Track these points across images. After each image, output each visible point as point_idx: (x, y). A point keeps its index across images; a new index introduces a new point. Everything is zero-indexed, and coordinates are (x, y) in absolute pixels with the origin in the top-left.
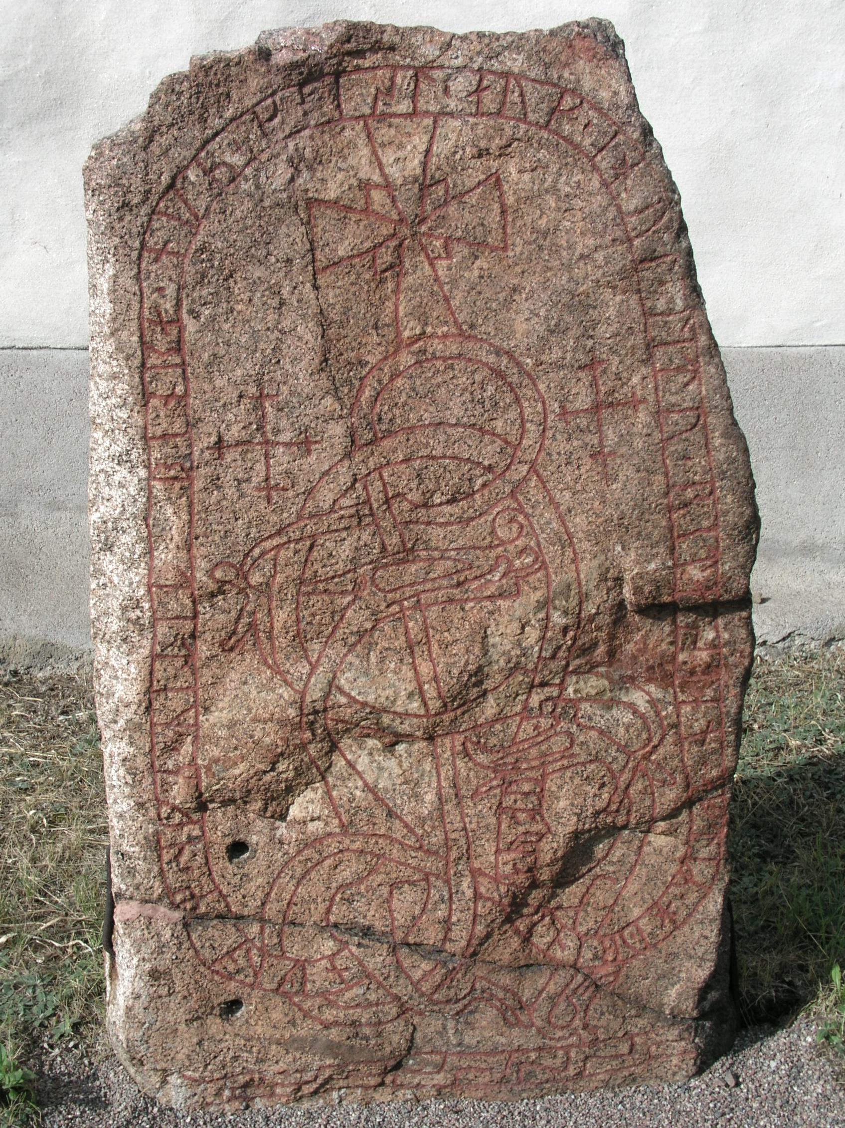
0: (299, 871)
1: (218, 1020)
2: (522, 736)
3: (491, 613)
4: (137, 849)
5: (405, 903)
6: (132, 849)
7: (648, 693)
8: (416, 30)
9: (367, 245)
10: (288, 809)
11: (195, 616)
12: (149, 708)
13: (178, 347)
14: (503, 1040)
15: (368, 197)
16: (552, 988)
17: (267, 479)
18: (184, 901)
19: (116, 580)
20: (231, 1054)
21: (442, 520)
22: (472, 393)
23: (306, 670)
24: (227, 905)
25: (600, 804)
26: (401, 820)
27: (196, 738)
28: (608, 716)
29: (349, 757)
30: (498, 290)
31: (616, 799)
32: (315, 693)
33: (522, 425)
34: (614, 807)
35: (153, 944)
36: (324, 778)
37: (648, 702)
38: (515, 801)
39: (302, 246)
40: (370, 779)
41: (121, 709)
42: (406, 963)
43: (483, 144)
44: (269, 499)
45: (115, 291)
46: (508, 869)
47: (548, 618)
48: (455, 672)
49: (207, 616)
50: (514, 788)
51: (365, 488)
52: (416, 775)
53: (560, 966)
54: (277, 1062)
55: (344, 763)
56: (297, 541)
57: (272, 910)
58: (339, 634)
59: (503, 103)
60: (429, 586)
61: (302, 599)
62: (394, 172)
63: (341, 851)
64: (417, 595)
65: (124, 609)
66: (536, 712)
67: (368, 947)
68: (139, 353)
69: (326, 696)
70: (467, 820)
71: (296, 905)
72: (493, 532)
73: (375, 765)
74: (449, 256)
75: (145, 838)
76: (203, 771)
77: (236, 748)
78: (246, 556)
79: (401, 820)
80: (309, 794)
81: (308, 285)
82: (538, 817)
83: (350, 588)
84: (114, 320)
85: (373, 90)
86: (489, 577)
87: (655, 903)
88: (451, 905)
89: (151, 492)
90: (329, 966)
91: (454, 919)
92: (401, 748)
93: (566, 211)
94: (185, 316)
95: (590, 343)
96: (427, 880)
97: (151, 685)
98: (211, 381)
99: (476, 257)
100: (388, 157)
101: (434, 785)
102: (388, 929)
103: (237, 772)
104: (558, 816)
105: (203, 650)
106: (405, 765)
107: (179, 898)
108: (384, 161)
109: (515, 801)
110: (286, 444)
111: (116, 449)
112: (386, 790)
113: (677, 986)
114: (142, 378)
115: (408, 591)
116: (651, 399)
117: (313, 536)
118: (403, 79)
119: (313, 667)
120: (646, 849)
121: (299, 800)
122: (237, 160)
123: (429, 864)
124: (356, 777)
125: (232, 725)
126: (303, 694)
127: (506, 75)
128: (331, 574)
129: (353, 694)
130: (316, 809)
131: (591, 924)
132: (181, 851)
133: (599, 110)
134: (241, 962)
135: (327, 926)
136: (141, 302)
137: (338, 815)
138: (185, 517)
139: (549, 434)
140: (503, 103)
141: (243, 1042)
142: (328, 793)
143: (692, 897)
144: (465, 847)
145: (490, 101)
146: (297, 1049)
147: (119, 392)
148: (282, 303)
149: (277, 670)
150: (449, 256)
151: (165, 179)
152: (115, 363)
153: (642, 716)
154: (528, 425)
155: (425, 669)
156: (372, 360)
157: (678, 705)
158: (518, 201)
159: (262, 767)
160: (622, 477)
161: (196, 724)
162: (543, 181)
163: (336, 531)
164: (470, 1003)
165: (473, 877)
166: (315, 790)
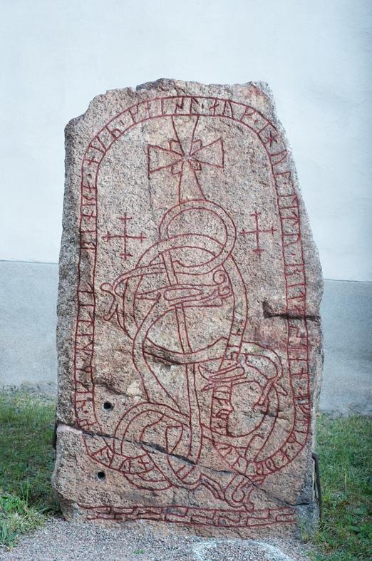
14: (211, 504)
16: (235, 483)
19: (66, 289)
24: (101, 429)
28: (259, 362)
31: (263, 399)
34: (261, 403)
41: (65, 342)
42: (172, 463)
50: (218, 389)
57: (119, 434)
58: (149, 316)
60: (187, 299)
64: (182, 303)
66: (229, 357)
69: (143, 342)
78: (115, 281)
87: (281, 450)
89: (80, 254)
104: (236, 404)
111: (69, 237)
115: (179, 301)
129: (154, 341)
131: (252, 456)
132: (84, 404)
141: (103, 491)
143: (296, 450)
157: (289, 360)
161: (93, 351)
166: (138, 382)
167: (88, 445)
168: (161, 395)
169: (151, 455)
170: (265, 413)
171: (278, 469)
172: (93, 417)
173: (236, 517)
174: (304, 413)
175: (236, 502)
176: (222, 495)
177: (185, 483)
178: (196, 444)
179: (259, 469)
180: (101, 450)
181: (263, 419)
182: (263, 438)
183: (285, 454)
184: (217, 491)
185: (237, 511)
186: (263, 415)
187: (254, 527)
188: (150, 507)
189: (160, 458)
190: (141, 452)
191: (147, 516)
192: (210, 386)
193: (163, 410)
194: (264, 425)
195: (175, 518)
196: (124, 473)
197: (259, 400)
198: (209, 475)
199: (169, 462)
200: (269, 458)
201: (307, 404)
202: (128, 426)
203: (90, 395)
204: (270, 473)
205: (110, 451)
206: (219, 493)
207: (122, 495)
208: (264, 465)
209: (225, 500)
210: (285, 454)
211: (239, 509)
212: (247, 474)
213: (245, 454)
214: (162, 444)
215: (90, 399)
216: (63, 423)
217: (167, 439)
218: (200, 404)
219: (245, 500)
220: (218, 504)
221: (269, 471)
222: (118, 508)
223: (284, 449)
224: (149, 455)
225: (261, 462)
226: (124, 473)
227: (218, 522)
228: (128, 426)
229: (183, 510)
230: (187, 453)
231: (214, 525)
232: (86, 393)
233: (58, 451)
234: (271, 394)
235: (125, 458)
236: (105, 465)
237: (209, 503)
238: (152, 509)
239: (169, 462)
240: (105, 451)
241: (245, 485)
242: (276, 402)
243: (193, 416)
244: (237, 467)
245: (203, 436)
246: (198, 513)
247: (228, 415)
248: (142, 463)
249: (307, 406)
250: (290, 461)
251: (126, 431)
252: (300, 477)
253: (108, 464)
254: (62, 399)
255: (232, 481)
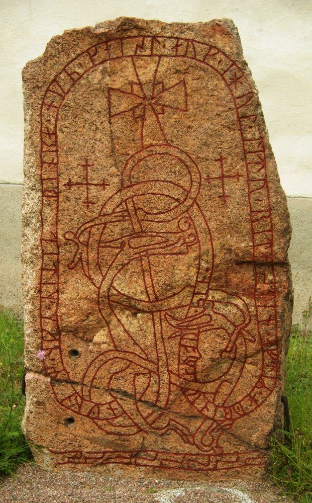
0: (97, 366)
1: (63, 426)
2: (189, 315)
3: (176, 260)
4: (34, 349)
5: (142, 381)
6: (32, 349)
7: (243, 301)
8: (152, 21)
9: (131, 107)
10: (93, 337)
11: (58, 254)
12: (40, 291)
13: (55, 144)
14: (181, 448)
15: (132, 88)
17: (87, 198)
18: (51, 373)
19: (30, 237)
20: (68, 442)
21: (157, 220)
22: (171, 168)
23: (101, 278)
24: (69, 376)
25: (223, 347)
26: (139, 346)
27: (58, 304)
28: (226, 309)
29: (118, 318)
30: (183, 127)
31: (230, 345)
32: (105, 288)
33: (191, 184)
34: (229, 349)
35: (38, 390)
36: (108, 325)
37: (243, 304)
38: (186, 342)
39: (105, 106)
40: (126, 328)
41: (30, 290)
42: (141, 409)
43: (178, 68)
44: (88, 207)
45: (32, 120)
46: (183, 371)
47: (199, 264)
48: (161, 283)
49: (63, 254)
50: (186, 337)
51: (126, 204)
52: (145, 327)
53: (207, 418)
54: (87, 447)
55: (116, 320)
56: (99, 225)
57: (87, 380)
58: (114, 265)
59: (187, 51)
60: (151, 247)
61: (100, 249)
62: (143, 78)
63: (115, 358)
64: (146, 251)
65: (32, 249)
66: (196, 305)
67: (124, 400)
68: (40, 146)
69: (109, 290)
70: (166, 348)
71: (96, 379)
72: (179, 227)
73: (129, 322)
74: (163, 113)
75: (37, 345)
76: (59, 318)
77: (72, 309)
78: (78, 229)
79: (139, 346)
80: (102, 332)
81: (107, 122)
82: (196, 351)
83: (119, 245)
84: (31, 132)
85: (135, 46)
86: (176, 245)
87: (249, 395)
88: (159, 386)
89: (43, 202)
90: (109, 407)
91: (160, 391)
92: (139, 315)
93: (211, 96)
94: (58, 132)
95: (220, 150)
96: (150, 373)
97: (41, 281)
98: (67, 158)
99: (174, 114)
100: (140, 72)
101: (153, 332)
102: (133, 393)
103: (72, 319)
104: (204, 351)
105: (61, 269)
106: (141, 323)
107: (49, 371)
108: (139, 74)
109: (186, 342)
110: (95, 185)
111: (31, 184)
112: (133, 333)
113: (257, 433)
114: (41, 156)
115: (143, 249)
116: (245, 174)
117: (105, 223)
118: (148, 42)
119: (104, 277)
120: (244, 370)
121: (98, 334)
122: (81, 71)
123: (150, 366)
124: (121, 326)
125: (71, 300)
126: (99, 288)
127: (187, 40)
128: (112, 239)
129: (119, 290)
130: (105, 339)
131: (220, 401)
132: (51, 351)
133: (225, 55)
134: (74, 402)
135: (108, 390)
136: (41, 125)
137: (113, 342)
138: (55, 212)
139: (202, 187)
140: (187, 51)
141: (73, 437)
142: (109, 332)
143: (265, 394)
144: (166, 360)
145: (181, 51)
146: (95, 442)
147: (32, 161)
148: (97, 128)
149: (90, 278)
150: (163, 113)
151: (52, 77)
152: (31, 149)
153: (241, 310)
154: (193, 183)
155: (148, 282)
156: (131, 153)
157: (256, 307)
158: (192, 91)
159: (82, 318)
160: (231, 207)
161: (58, 299)
162: (202, 84)
163: (114, 222)
164: (167, 431)
165: (169, 374)
166: (104, 330)
167: (56, 392)
168: (127, 343)
169: (119, 401)
170: (234, 359)
171: (245, 414)
172: (60, 364)
173: (205, 461)
174: (273, 359)
175: (206, 446)
176: (191, 440)
177: (154, 428)
178: (164, 391)
179: (226, 413)
180: (69, 397)
181: (232, 364)
182: (231, 383)
183: (253, 399)
184: (186, 435)
185: (206, 455)
186: (231, 361)
187: (224, 471)
188: (121, 452)
189: (128, 405)
190: (109, 399)
191: (118, 460)
192: (177, 334)
193: (131, 357)
194: (232, 371)
195: (145, 462)
196: (93, 419)
197: (227, 347)
198: (178, 420)
199: (137, 408)
200: (237, 403)
201: (275, 350)
202: (96, 373)
203: (57, 344)
204: (238, 418)
205: (78, 398)
206: (186, 437)
207: (92, 440)
208: (233, 410)
209: (194, 444)
210: (253, 399)
211: (208, 453)
212: (217, 418)
213: (214, 399)
214: (130, 391)
215: (56, 348)
216: (31, 370)
217: (134, 385)
218: (168, 352)
219: (214, 445)
220: (187, 448)
221: (238, 416)
222: (89, 453)
223: (253, 394)
224: (117, 402)
225: (229, 407)
226: (93, 419)
227: (188, 466)
228: (96, 373)
229: (153, 454)
230: (155, 399)
231: (183, 468)
232: (53, 340)
233: (27, 397)
234: (239, 341)
235: (94, 405)
236: (73, 411)
237: (178, 447)
238: (122, 454)
239: (137, 408)
240: (73, 398)
241: (214, 430)
242: (244, 348)
243: (161, 363)
244: (205, 412)
245: (170, 383)
246: (167, 457)
247: (195, 362)
248: (111, 408)
249: (275, 352)
250: (258, 406)
251: (94, 378)
252: (268, 422)
253: (77, 410)
254: (29, 346)
255: (201, 426)
